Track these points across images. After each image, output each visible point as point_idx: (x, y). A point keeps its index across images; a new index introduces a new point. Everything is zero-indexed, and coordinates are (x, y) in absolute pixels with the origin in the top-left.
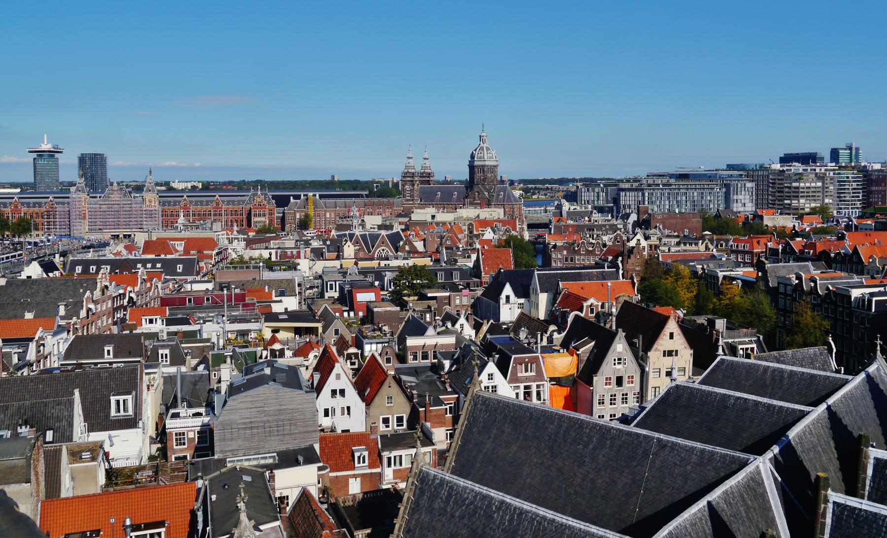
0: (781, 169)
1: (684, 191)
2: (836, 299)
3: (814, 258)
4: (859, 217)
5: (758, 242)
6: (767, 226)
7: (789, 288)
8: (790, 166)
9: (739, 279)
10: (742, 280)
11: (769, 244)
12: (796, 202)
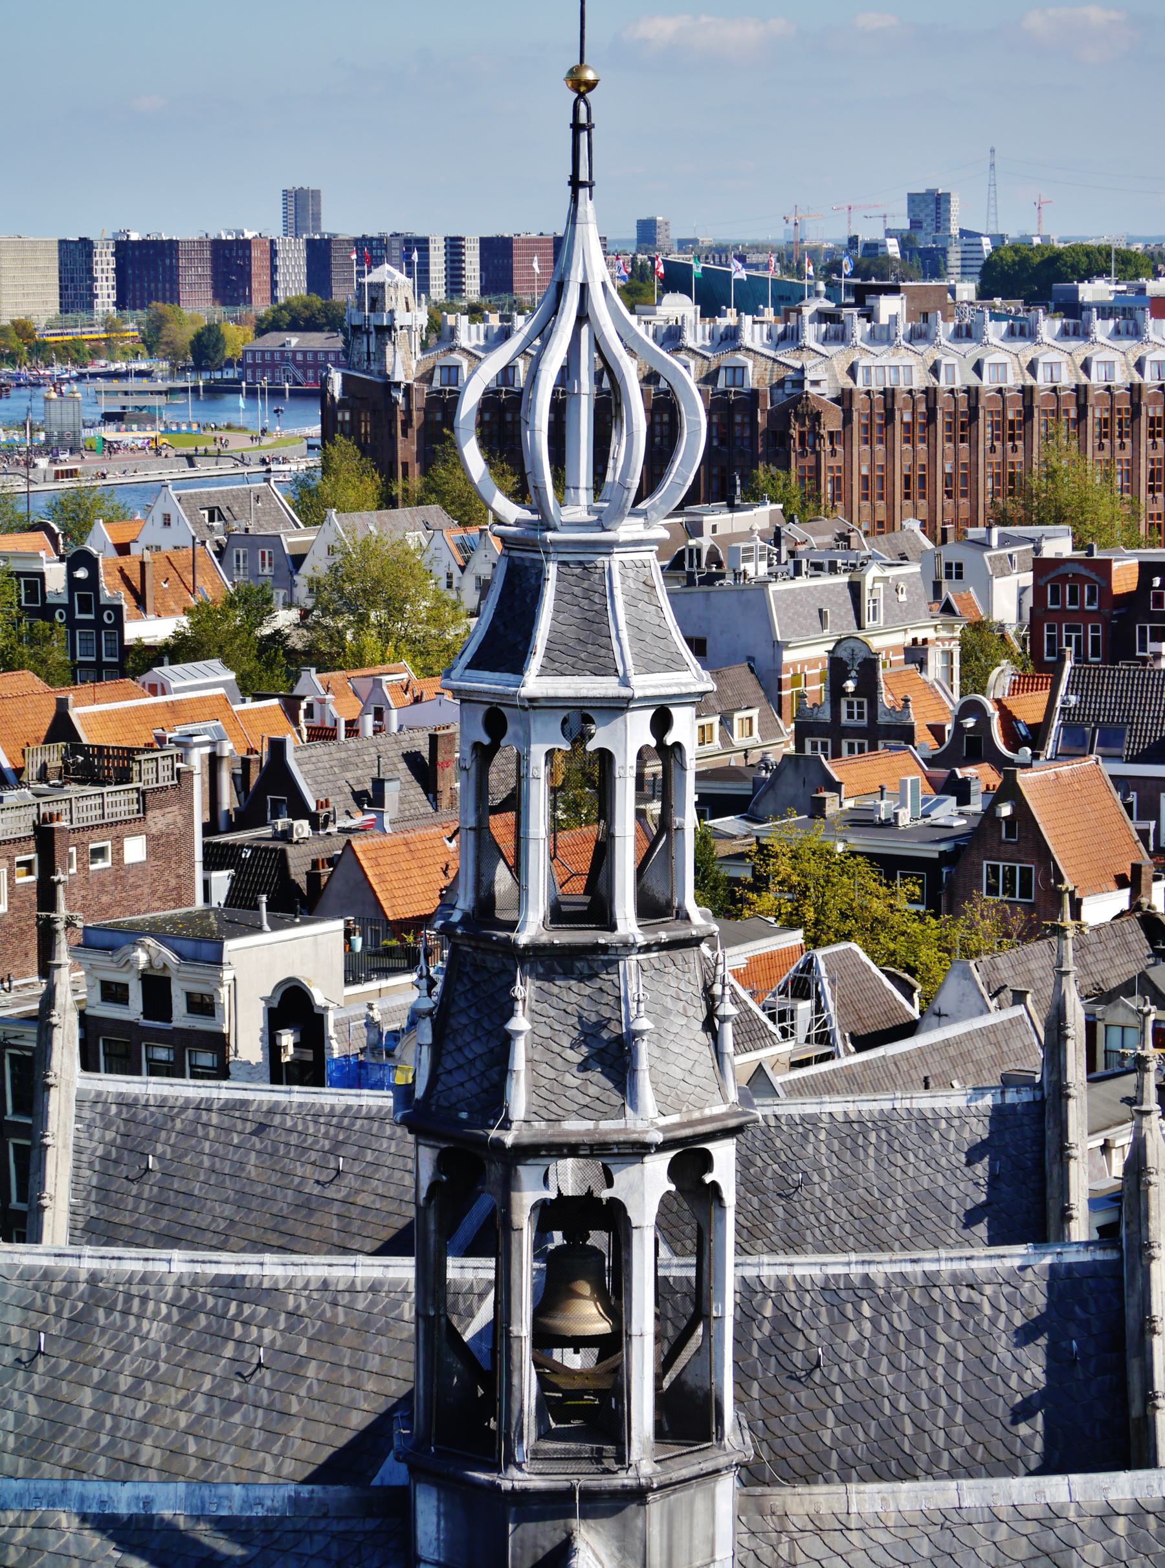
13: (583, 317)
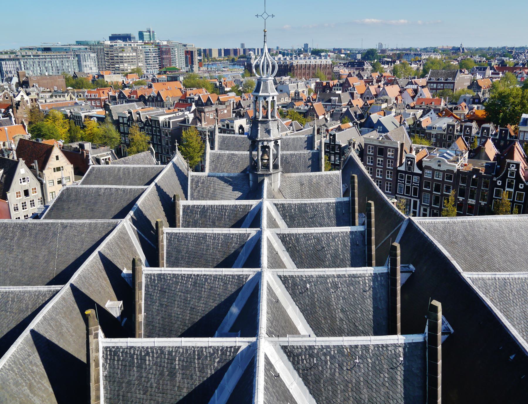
0: (111, 44)
1: (50, 60)
2: (152, 123)
3: (137, 100)
4: (159, 74)
5: (103, 92)
6: (107, 81)
7: (125, 119)
8: (116, 42)
9: (94, 117)
10: (97, 117)
11: (110, 93)
12: (122, 65)
13: (265, 56)
